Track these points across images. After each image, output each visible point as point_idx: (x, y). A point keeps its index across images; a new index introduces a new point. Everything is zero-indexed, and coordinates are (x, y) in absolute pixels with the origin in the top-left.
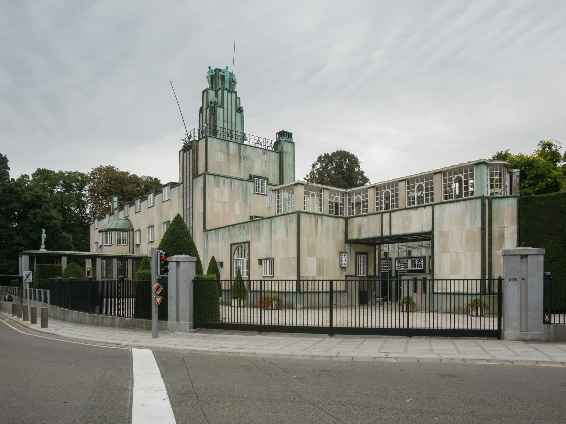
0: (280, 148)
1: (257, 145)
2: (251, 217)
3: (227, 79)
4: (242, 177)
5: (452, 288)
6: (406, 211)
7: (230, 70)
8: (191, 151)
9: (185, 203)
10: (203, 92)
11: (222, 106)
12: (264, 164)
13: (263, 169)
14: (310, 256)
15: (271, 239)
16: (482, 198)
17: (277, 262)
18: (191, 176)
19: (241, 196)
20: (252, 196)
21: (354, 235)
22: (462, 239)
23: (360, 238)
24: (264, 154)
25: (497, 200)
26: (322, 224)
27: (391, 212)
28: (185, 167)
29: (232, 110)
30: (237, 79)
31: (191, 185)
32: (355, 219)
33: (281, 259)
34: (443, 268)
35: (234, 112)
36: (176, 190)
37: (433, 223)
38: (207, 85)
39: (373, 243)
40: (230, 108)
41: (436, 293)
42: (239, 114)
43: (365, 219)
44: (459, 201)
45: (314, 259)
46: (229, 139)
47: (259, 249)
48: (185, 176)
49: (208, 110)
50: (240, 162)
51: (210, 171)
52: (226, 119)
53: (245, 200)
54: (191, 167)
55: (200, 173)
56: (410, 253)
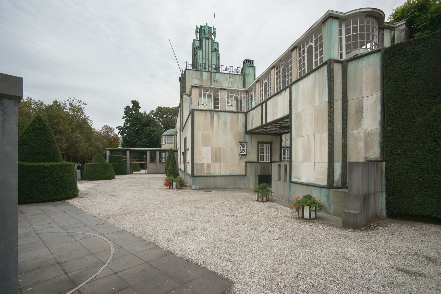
1: (226, 72)
3: (207, 31)
7: (209, 25)
12: (230, 84)
14: (205, 146)
26: (218, 119)
29: (209, 51)
35: (210, 52)
40: (207, 50)
45: (210, 148)
52: (204, 57)
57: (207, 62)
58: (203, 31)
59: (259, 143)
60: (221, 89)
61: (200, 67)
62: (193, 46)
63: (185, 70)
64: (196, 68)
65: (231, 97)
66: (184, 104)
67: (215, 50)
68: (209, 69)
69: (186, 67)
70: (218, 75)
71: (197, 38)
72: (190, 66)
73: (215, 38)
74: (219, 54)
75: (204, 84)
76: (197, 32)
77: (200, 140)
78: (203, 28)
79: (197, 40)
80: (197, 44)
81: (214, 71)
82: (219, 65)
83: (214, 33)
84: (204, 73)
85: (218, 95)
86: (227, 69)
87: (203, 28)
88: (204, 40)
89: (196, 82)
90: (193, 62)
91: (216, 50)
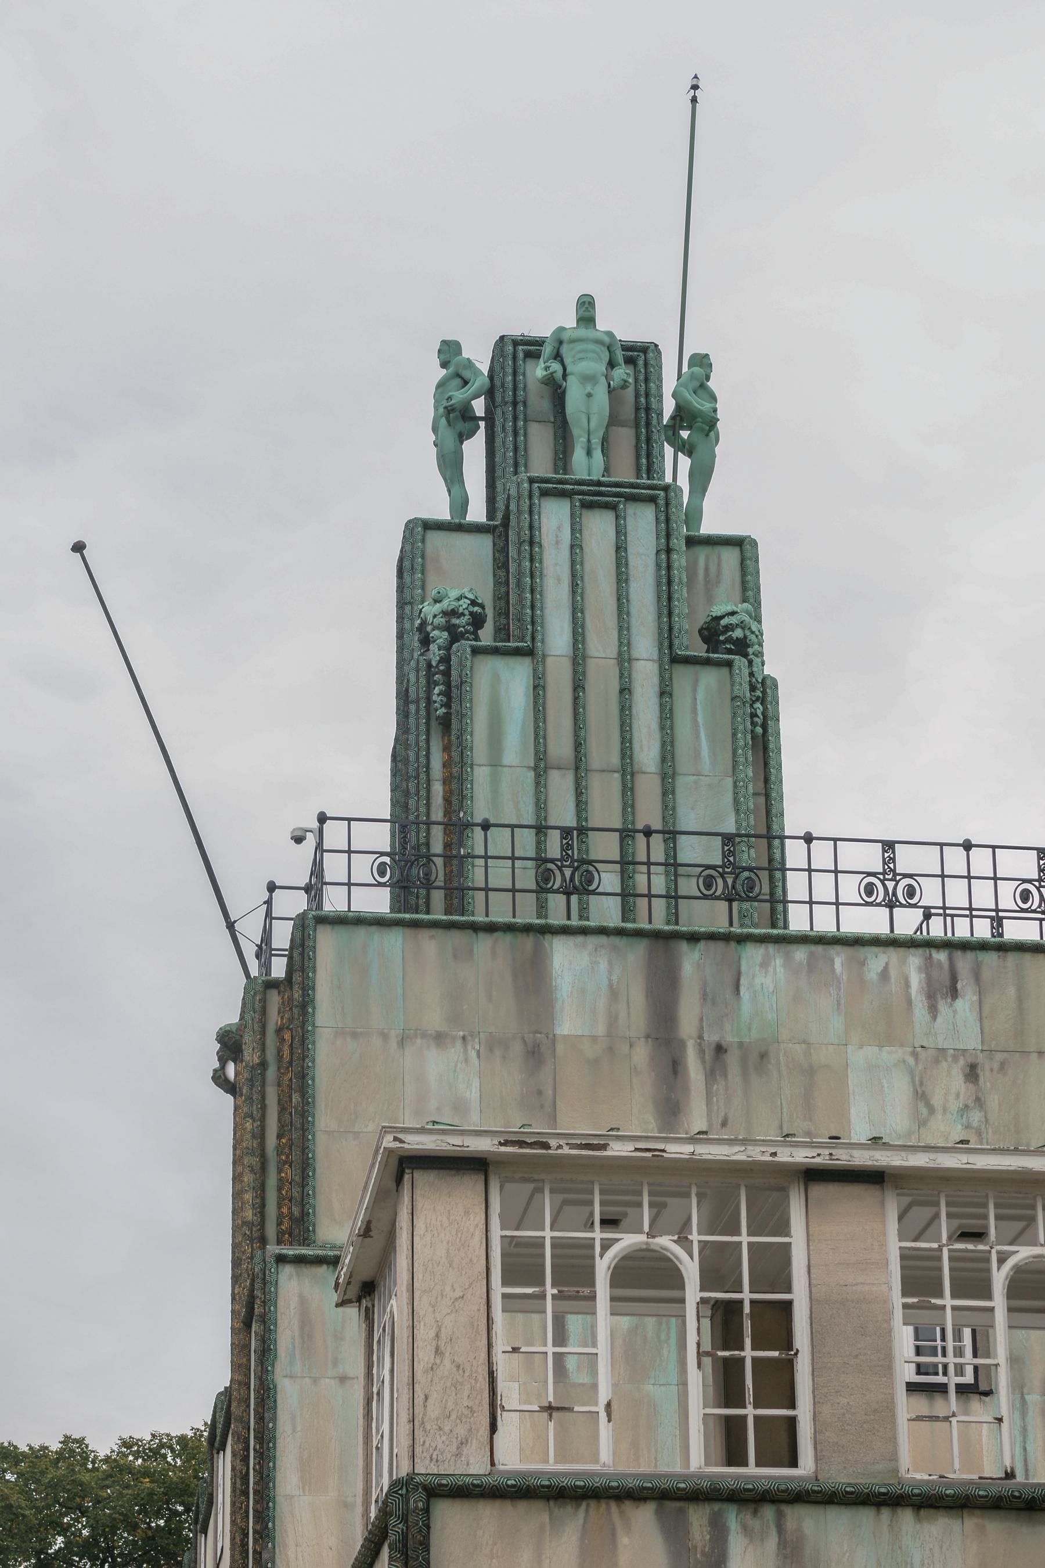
1: (871, 921)
3: (588, 403)
7: (619, 323)
11: (519, 640)
12: (949, 1086)
29: (624, 660)
40: (601, 647)
52: (561, 746)
57: (606, 810)
58: (539, 403)
60: (813, 1176)
61: (500, 875)
62: (404, 603)
63: (309, 925)
64: (457, 894)
65: (973, 1283)
66: (289, 1392)
67: (712, 633)
68: (627, 895)
69: (314, 889)
70: (766, 976)
71: (461, 504)
72: (363, 869)
73: (701, 477)
74: (762, 694)
75: (574, 1122)
76: (456, 420)
78: (537, 371)
79: (458, 527)
80: (464, 573)
81: (708, 915)
82: (771, 836)
83: (696, 424)
85: (774, 1268)
86: (888, 885)
87: (537, 371)
88: (554, 518)
89: (459, 1095)
90: (405, 817)
91: (728, 644)
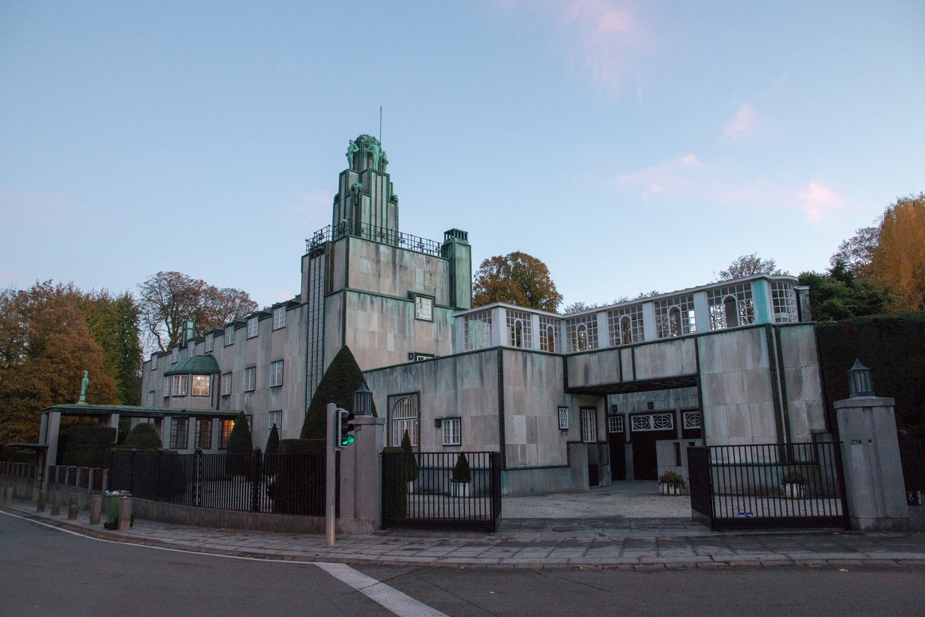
0: (449, 253)
2: (411, 355)
4: (397, 295)
5: (735, 457)
6: (657, 345)
8: (323, 257)
9: (310, 333)
10: (341, 175)
12: (428, 275)
13: (427, 283)
15: (456, 389)
16: (767, 326)
17: (466, 421)
18: (322, 293)
19: (396, 324)
20: (412, 324)
21: (578, 381)
22: (743, 386)
23: (588, 385)
24: (428, 262)
25: (787, 329)
26: (533, 365)
27: (633, 347)
28: (312, 279)
30: (388, 158)
31: (321, 306)
32: (577, 357)
33: (474, 419)
34: (720, 429)
36: (295, 313)
37: (698, 362)
38: (345, 165)
39: (602, 392)
40: (379, 198)
41: (714, 465)
42: (393, 205)
43: (594, 358)
44: (734, 330)
46: (378, 240)
47: (436, 402)
48: (312, 293)
49: (349, 199)
50: (394, 274)
51: (351, 286)
52: (373, 213)
53: (402, 330)
54: (322, 280)
55: (336, 289)
56: (651, 405)
59: (581, 408)
77: (512, 401)
84: (383, 248)
